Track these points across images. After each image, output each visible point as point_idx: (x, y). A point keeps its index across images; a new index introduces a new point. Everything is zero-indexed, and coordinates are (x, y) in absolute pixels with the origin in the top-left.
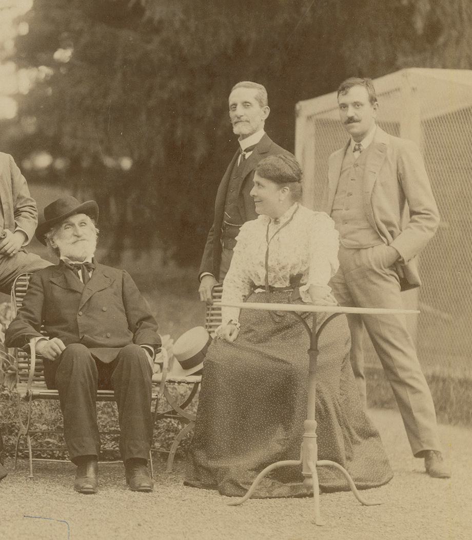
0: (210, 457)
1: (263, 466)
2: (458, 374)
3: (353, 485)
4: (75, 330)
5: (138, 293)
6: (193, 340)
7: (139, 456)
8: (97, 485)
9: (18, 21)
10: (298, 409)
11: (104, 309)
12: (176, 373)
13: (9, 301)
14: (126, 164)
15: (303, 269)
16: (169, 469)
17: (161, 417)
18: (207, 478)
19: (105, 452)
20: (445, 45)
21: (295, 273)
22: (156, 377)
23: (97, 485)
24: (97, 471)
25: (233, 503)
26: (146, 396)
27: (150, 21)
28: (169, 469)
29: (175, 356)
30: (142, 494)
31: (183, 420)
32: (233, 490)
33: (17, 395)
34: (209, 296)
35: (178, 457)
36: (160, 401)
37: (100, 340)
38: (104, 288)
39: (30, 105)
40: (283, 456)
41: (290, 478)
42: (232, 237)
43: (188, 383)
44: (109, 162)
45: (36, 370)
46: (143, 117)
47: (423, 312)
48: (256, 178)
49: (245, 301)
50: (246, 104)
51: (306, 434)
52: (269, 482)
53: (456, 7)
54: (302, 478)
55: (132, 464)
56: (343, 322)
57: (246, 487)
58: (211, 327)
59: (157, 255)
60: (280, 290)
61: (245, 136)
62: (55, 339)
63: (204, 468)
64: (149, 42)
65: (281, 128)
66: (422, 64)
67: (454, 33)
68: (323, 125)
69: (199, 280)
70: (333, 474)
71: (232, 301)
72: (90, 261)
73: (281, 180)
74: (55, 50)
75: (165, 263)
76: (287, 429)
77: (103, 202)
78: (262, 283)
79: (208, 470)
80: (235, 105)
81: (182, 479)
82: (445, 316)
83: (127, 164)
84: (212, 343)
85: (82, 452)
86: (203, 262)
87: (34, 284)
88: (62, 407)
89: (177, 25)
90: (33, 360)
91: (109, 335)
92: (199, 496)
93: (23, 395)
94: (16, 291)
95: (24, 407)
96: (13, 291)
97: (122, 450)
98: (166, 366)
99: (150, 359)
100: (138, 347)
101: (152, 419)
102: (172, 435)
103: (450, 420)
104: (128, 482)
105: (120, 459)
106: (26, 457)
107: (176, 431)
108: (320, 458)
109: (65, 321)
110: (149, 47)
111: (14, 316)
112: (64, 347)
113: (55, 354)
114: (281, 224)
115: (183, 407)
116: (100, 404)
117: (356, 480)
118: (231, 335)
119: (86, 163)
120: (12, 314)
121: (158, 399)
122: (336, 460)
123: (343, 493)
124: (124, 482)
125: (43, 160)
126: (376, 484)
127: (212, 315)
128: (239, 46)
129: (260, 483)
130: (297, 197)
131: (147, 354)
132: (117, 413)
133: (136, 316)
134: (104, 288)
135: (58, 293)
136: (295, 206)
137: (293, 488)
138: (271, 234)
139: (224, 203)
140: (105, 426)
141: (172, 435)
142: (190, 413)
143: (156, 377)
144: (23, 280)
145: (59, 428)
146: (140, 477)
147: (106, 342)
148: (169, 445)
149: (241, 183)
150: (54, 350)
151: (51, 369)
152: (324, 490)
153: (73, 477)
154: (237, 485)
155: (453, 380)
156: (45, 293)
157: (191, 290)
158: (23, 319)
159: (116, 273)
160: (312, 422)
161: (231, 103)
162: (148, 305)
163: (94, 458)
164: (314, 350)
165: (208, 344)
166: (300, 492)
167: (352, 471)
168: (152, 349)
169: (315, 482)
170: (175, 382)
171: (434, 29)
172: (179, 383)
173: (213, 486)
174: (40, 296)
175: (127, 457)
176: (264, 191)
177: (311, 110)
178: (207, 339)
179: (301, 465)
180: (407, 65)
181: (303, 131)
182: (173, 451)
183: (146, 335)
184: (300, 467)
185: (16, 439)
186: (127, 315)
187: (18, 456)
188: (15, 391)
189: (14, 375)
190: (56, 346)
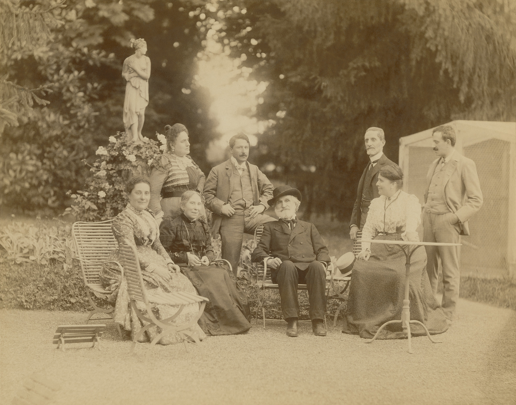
0: (355, 319)
1: (382, 323)
2: (481, 276)
3: (428, 332)
4: (287, 254)
5: (319, 235)
6: (346, 259)
7: (319, 318)
8: (298, 333)
9: (258, 97)
10: (400, 295)
11: (302, 243)
12: (338, 276)
13: (253, 239)
14: (313, 169)
15: (403, 224)
16: (335, 325)
17: (331, 298)
18: (354, 329)
19: (302, 315)
20: (475, 108)
21: (399, 225)
22: (328, 278)
23: (298, 333)
24: (298, 325)
25: (367, 342)
26: (323, 289)
27: (326, 97)
28: (335, 325)
29: (337, 267)
30: (321, 337)
31: (342, 300)
32: (367, 335)
33: (257, 287)
34: (355, 236)
35: (339, 318)
36: (330, 290)
37: (299, 259)
38: (301, 231)
39: (263, 140)
40: (393, 318)
41: (395, 330)
42: (367, 207)
43: (344, 281)
44: (304, 168)
45: (267, 274)
46: (322, 146)
47: (463, 244)
48: (380, 177)
49: (373, 239)
50: (373, 139)
51: (404, 307)
52: (385, 332)
53: (481, 89)
54: (402, 330)
55: (316, 322)
56: (422, 250)
57: (373, 334)
58: (356, 252)
59: (329, 215)
60: (391, 234)
61: (373, 156)
62: (277, 258)
63: (352, 324)
64: (325, 107)
65: (392, 151)
66: (464, 118)
67: (480, 103)
68: (413, 150)
69: (350, 228)
70: (418, 328)
71: (366, 240)
72: (295, 219)
73: (393, 178)
74: (278, 111)
75: (332, 219)
76: (394, 304)
77: (302, 189)
78: (382, 231)
79: (354, 325)
80: (368, 139)
81: (341, 329)
82: (475, 247)
83: (313, 169)
84: (356, 260)
85: (290, 316)
86: (352, 219)
87: (266, 230)
88: (280, 292)
89: (339, 99)
90: (265, 269)
91: (304, 256)
92: (350, 338)
93: (260, 287)
94: (257, 234)
95: (261, 293)
96: (255, 234)
97: (311, 315)
98: (333, 272)
99: (325, 269)
100: (318, 263)
101: (325, 300)
102: (336, 307)
103: (477, 300)
104: (314, 331)
105: (309, 319)
106: (262, 318)
107: (338, 305)
108: (411, 319)
109: (281, 249)
110: (325, 110)
111: (256, 246)
112: (281, 262)
113: (276, 266)
114: (391, 201)
115: (342, 293)
116: (299, 291)
117: (429, 330)
118: (366, 257)
119: (293, 168)
120: (255, 245)
121: (329, 289)
122: (419, 320)
123: (423, 337)
124: (312, 331)
125: (271, 167)
126: (440, 332)
127: (357, 246)
128: (371, 110)
129: (381, 332)
130: (400, 186)
131: (323, 266)
132: (308, 296)
133: (318, 247)
134: (301, 231)
135: (278, 235)
136: (399, 191)
137: (397, 335)
138: (386, 206)
139: (362, 189)
140: (302, 303)
141: (336, 307)
142: (345, 296)
143: (328, 278)
144: (260, 228)
145: (279, 303)
146: (320, 329)
147: (303, 260)
148: (334, 313)
149: (371, 179)
150: (276, 264)
151: (275, 274)
152: (413, 335)
153: (286, 328)
154: (367, 331)
155: (479, 279)
156: (271, 235)
157: (346, 233)
158: (260, 248)
159: (308, 224)
160: (407, 301)
161: (365, 139)
162: (324, 241)
163: (296, 319)
164: (408, 264)
165: (354, 261)
166: (401, 336)
167: (427, 326)
168: (326, 263)
169: (409, 331)
170: (337, 280)
171: (469, 101)
172: (340, 281)
173: (358, 333)
174: (269, 236)
175: (313, 319)
176: (383, 183)
177: (406, 142)
178: (354, 258)
179: (402, 322)
180: (456, 119)
181: (403, 153)
182: (336, 316)
183: (323, 257)
184: (401, 324)
185: (257, 309)
186: (313, 246)
187: (258, 318)
188: (256, 284)
189: (256, 276)
190: (277, 262)
